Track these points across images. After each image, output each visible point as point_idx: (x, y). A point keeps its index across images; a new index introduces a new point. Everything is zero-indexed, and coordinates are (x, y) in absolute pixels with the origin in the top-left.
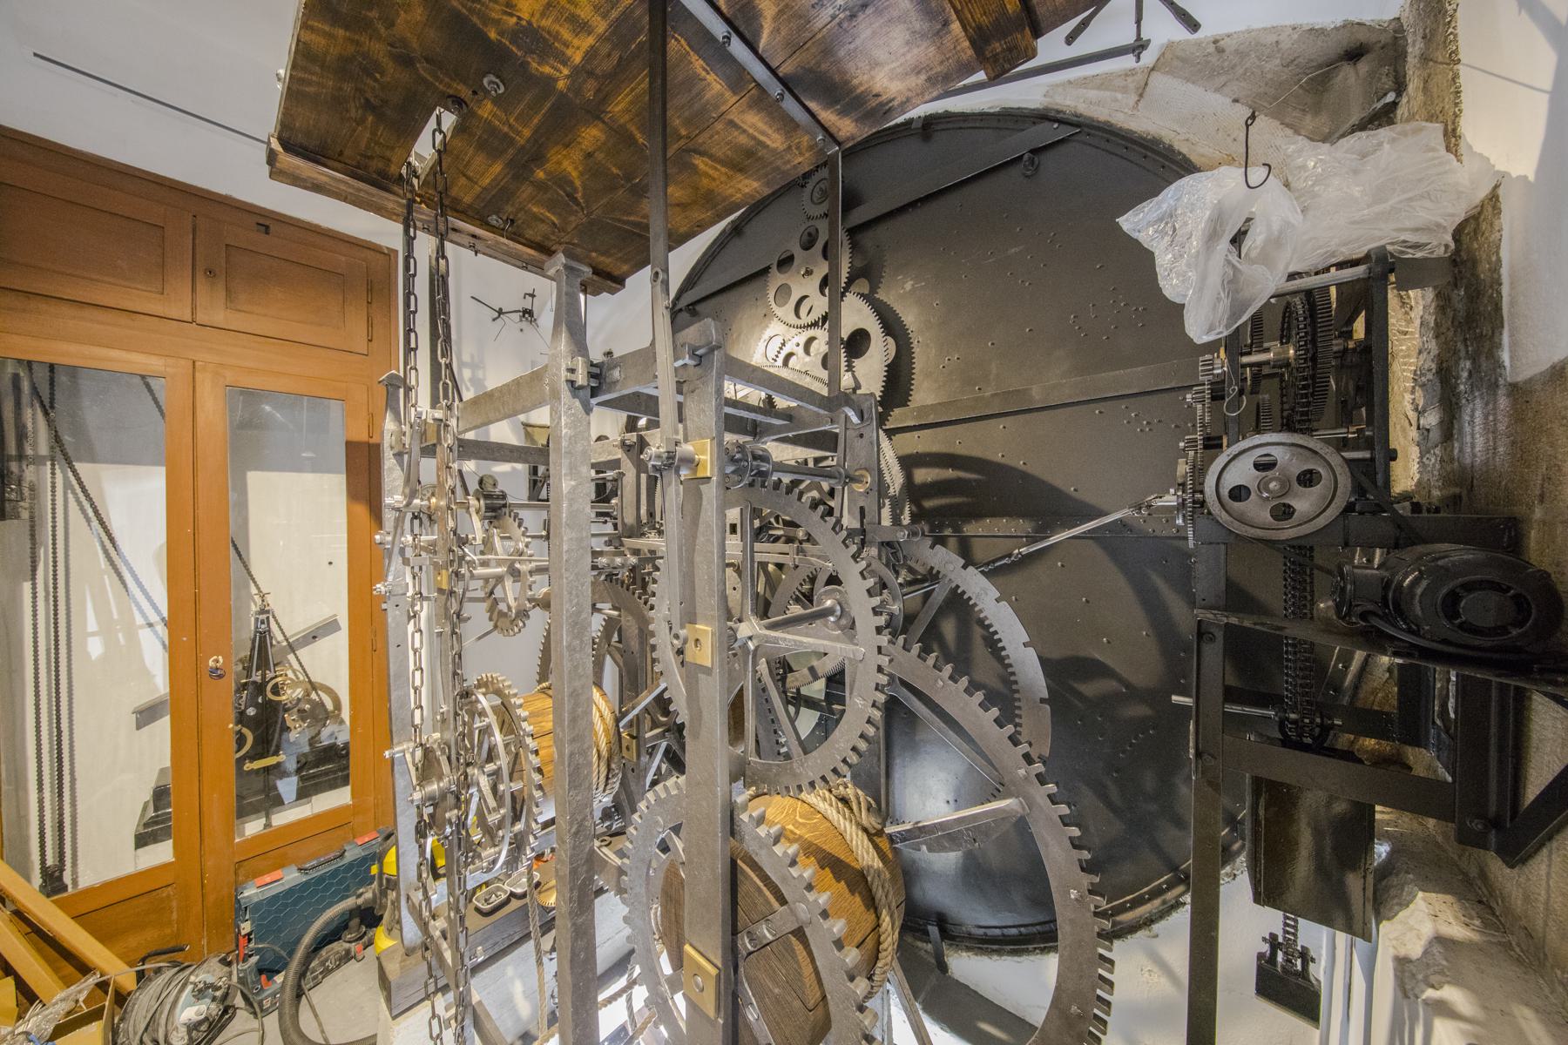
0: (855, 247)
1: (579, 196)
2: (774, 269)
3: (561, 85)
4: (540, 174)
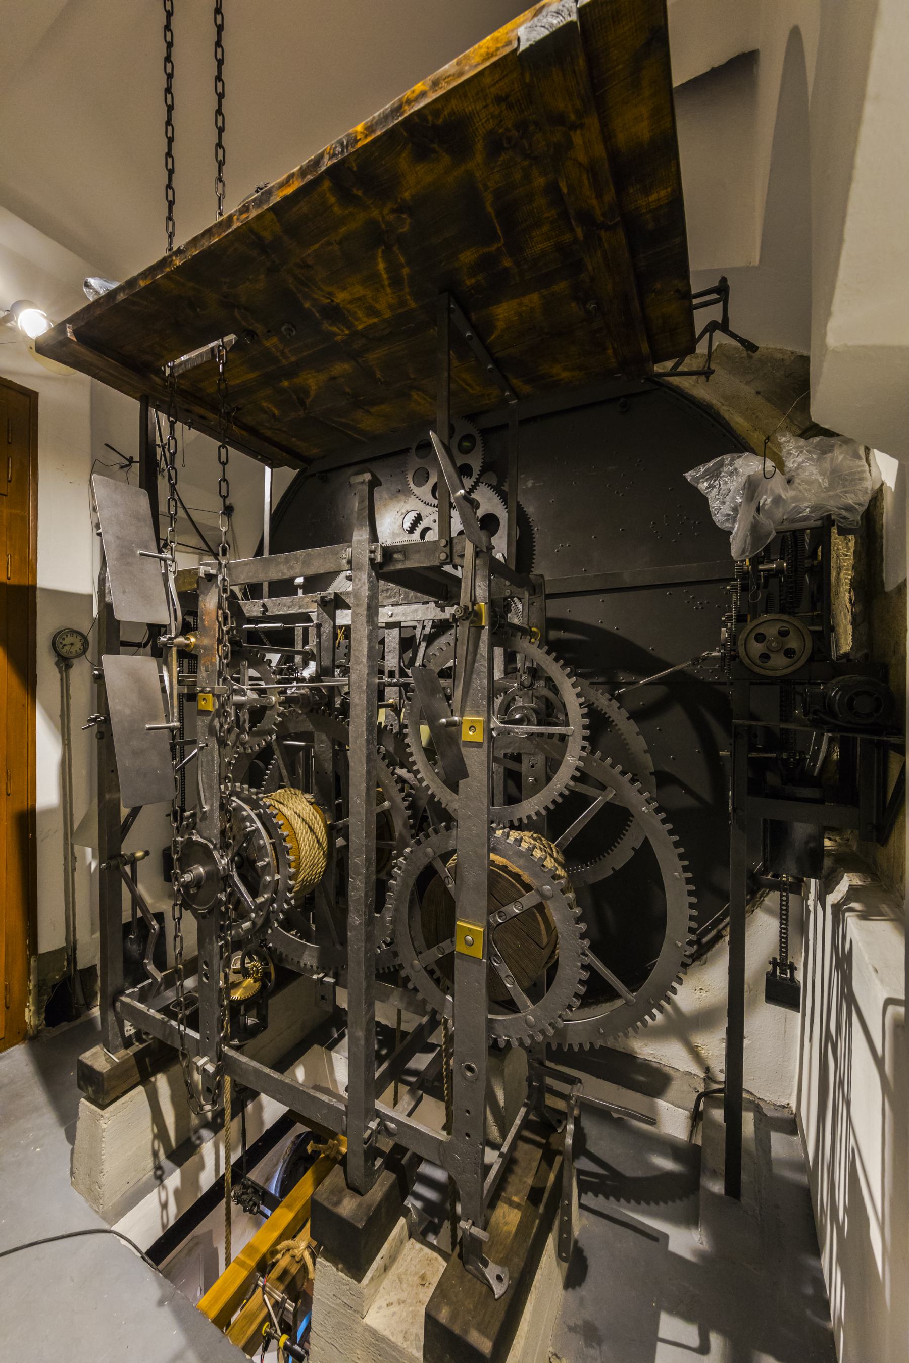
0: (485, 443)
1: (308, 401)
2: (413, 451)
3: (339, 338)
4: (286, 384)
